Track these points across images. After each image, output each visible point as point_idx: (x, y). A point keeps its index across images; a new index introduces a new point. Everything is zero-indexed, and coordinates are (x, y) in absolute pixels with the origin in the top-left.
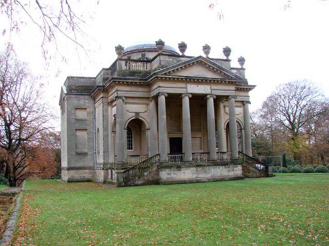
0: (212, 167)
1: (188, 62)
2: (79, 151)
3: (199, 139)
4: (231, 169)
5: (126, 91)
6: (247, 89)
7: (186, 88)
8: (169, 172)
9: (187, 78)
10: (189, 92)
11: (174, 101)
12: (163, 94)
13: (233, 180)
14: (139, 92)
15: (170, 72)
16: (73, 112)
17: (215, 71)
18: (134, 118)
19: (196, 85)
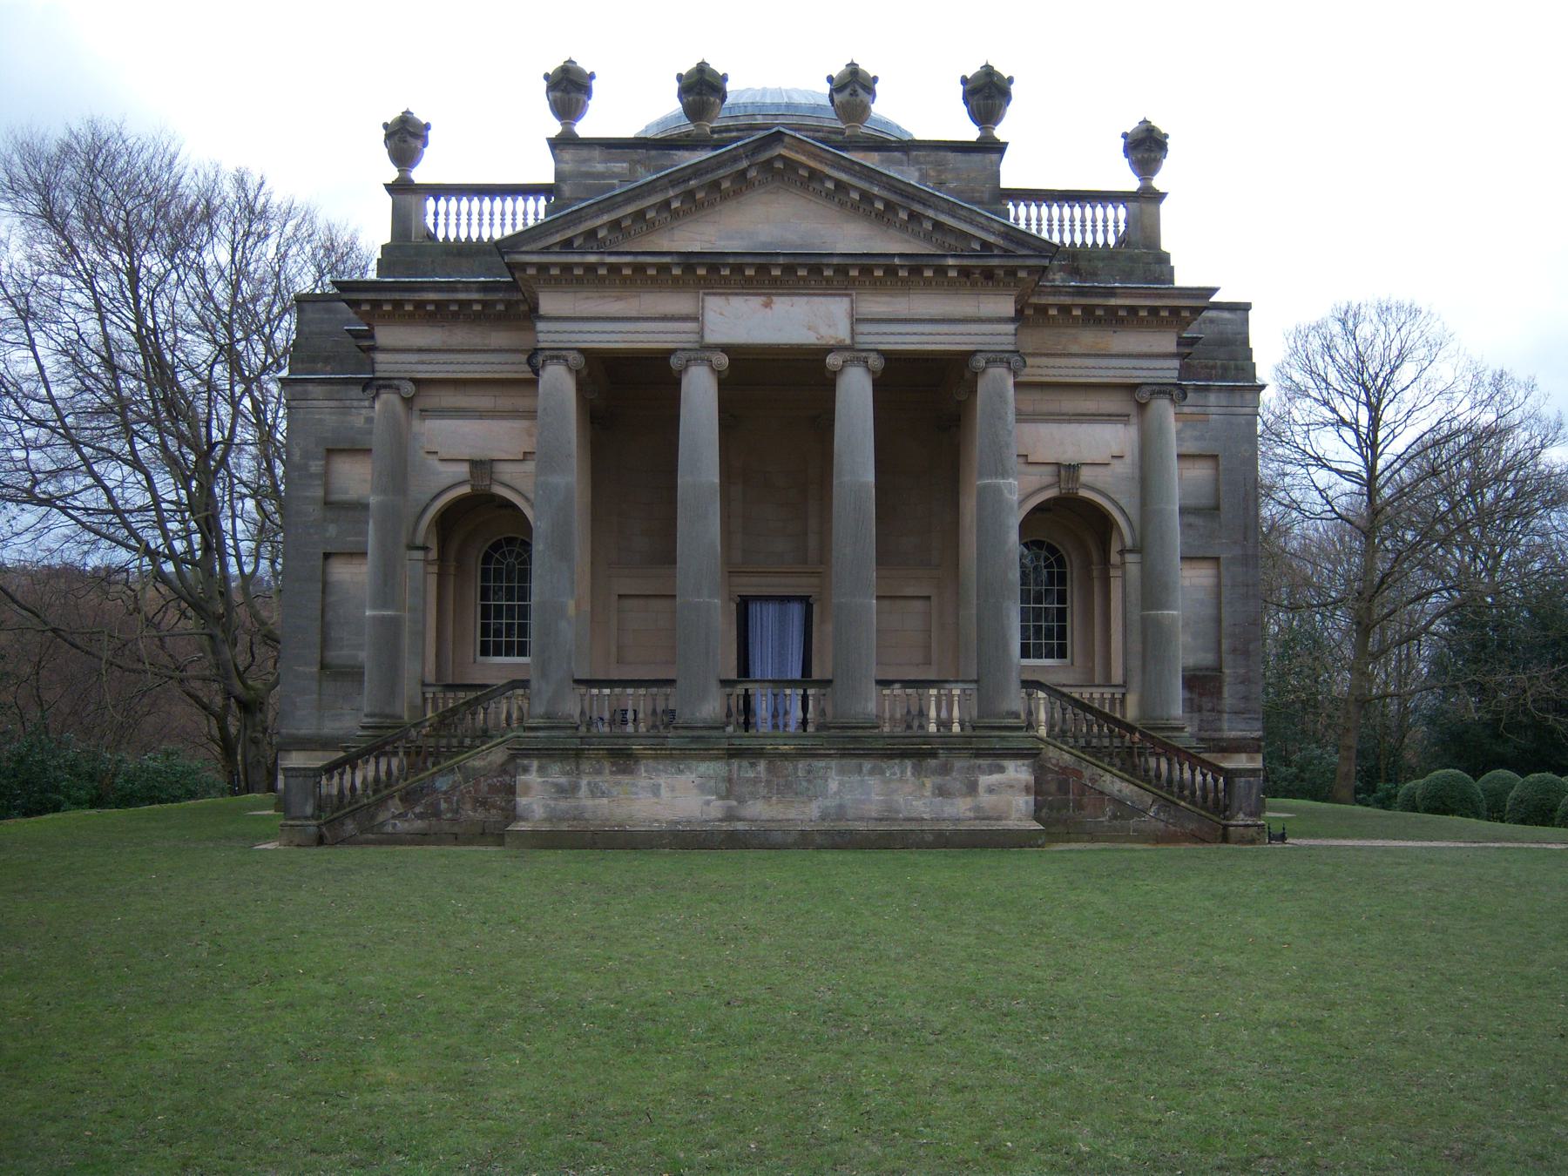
0: (834, 763)
1: (697, 170)
2: (337, 655)
3: (919, 605)
4: (955, 781)
5: (420, 350)
6: (1175, 311)
7: (695, 319)
8: (563, 780)
10: (710, 338)
12: (557, 355)
13: (930, 846)
15: (592, 233)
16: (316, 466)
17: (879, 216)
18: (466, 489)
19: (755, 302)
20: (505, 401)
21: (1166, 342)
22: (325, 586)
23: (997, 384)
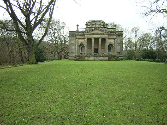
2: (72, 51)
9: (92, 34)
11: (89, 40)
14: (82, 37)
20: (83, 39)
21: (116, 36)
22: (71, 48)
23: (107, 39)
